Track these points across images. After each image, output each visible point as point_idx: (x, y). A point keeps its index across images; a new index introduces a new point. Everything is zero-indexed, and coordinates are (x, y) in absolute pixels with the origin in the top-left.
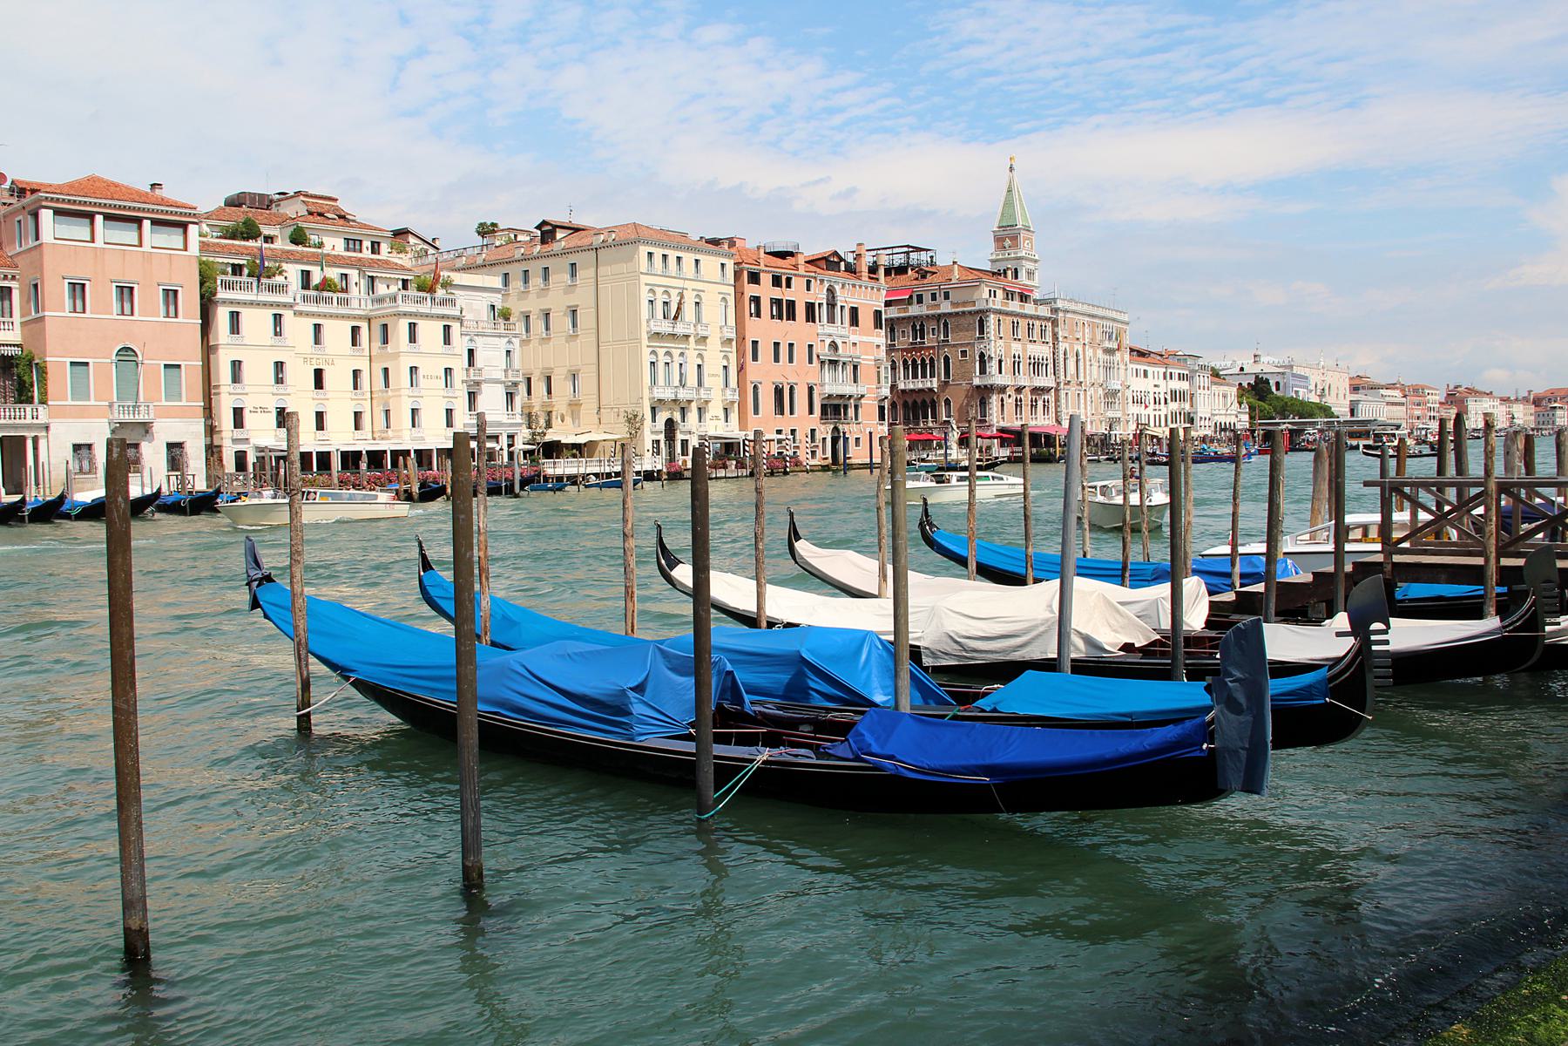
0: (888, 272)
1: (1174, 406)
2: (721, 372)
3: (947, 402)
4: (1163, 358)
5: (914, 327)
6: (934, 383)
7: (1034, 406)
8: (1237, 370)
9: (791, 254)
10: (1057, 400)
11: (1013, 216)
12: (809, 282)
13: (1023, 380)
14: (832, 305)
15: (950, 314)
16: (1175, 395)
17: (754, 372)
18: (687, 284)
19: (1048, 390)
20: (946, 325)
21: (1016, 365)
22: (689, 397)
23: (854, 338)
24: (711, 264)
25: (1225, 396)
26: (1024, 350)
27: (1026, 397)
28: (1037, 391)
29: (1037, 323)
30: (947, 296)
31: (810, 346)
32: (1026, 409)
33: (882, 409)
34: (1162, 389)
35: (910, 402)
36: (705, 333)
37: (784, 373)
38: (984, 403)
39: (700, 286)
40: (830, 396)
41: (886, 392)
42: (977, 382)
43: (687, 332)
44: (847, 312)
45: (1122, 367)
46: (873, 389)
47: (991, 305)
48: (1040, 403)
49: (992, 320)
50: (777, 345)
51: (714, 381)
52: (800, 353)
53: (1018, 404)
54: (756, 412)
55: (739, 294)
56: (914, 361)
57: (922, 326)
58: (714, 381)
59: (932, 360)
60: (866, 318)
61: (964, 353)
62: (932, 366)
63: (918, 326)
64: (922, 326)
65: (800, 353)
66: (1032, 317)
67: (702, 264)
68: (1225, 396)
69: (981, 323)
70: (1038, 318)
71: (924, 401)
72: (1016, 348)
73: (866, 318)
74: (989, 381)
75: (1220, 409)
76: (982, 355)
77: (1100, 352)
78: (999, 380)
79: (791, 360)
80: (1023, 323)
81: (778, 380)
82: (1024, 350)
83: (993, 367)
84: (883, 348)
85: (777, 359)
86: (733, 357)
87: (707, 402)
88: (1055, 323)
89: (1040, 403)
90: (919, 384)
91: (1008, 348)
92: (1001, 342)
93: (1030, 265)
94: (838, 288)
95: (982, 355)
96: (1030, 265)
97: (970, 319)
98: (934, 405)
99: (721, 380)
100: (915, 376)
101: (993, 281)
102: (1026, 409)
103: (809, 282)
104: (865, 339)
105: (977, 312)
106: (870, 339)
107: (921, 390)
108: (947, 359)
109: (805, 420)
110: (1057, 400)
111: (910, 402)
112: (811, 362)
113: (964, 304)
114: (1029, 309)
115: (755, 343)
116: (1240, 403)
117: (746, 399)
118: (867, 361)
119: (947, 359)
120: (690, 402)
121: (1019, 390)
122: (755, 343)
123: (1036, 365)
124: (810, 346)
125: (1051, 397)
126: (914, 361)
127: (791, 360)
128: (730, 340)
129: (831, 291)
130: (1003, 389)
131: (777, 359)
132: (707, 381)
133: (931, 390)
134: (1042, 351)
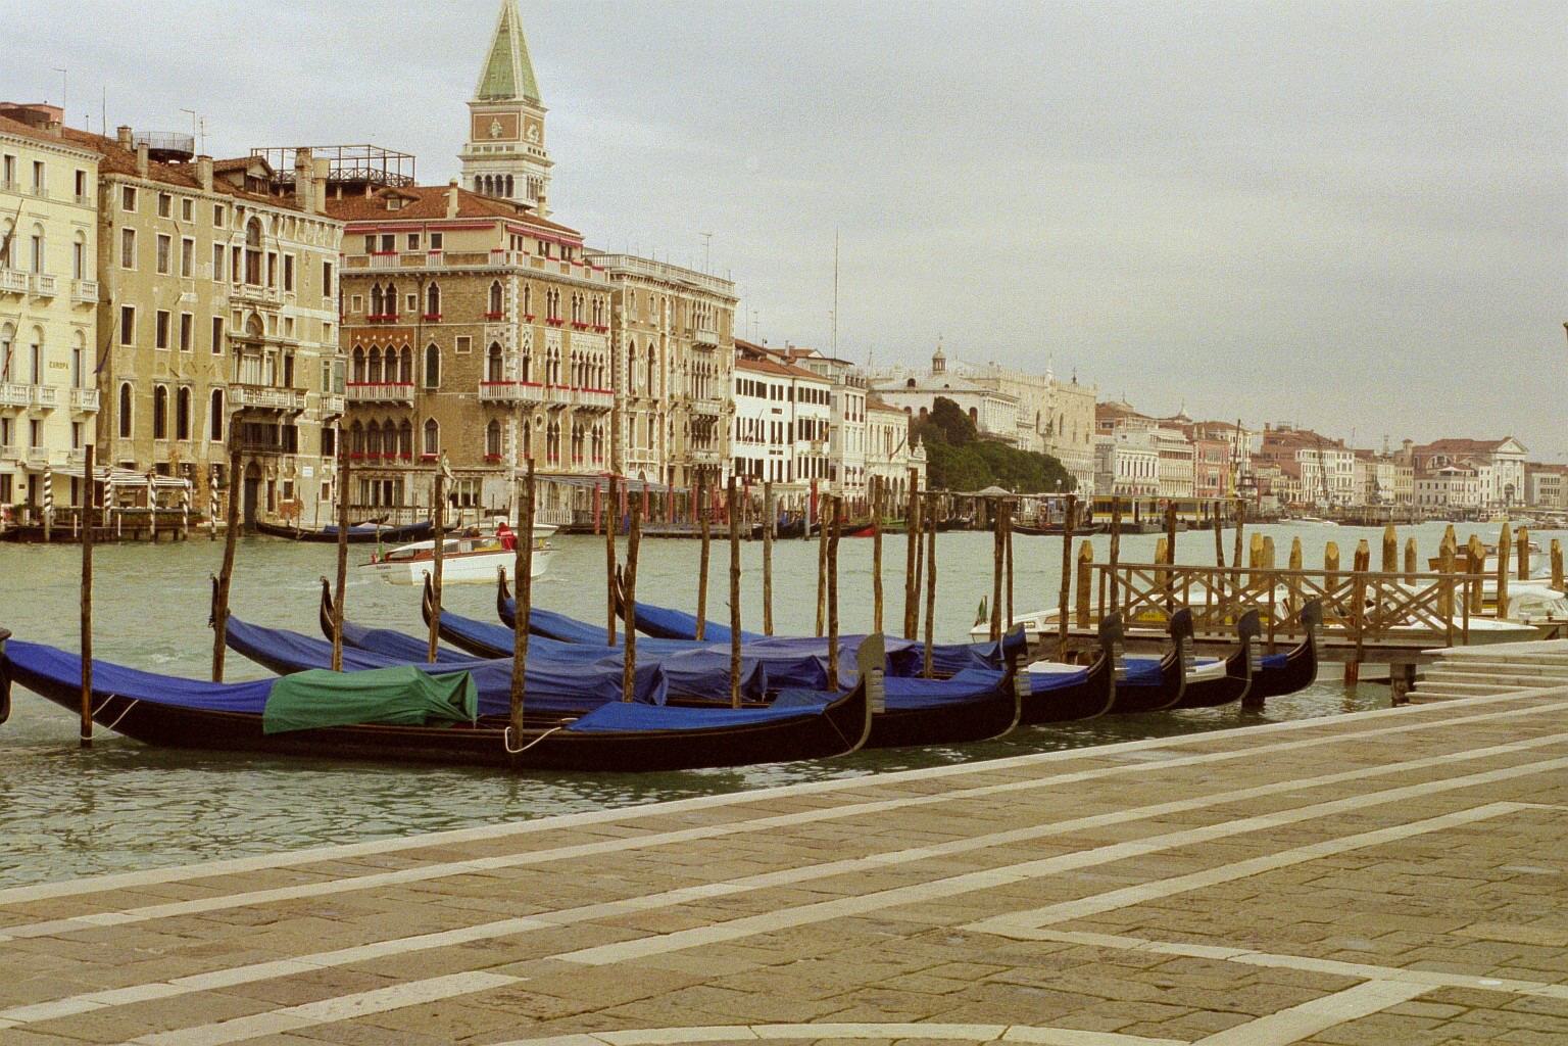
0: (331, 187)
1: (803, 446)
2: (70, 359)
3: (431, 426)
4: (789, 360)
5: (377, 291)
6: (410, 393)
7: (577, 439)
8: (902, 382)
9: (183, 156)
10: (615, 430)
11: (508, 76)
12: (219, 210)
13: (563, 397)
14: (253, 257)
15: (443, 274)
16: (807, 429)
17: (126, 364)
18: (30, 205)
19: (603, 411)
20: (434, 297)
21: (552, 364)
22: (18, 401)
23: (287, 310)
24: (61, 168)
25: (888, 433)
26: (566, 341)
27: (566, 423)
28: (583, 411)
29: (589, 296)
30: (437, 241)
31: (218, 322)
32: (565, 444)
33: (327, 434)
34: (785, 418)
35: (364, 421)
36: (47, 292)
37: (168, 367)
38: (494, 430)
39: (39, 207)
40: (248, 409)
41: (337, 404)
42: (484, 393)
43: (18, 288)
44: (280, 264)
45: (723, 377)
46: (317, 404)
47: (514, 261)
48: (588, 434)
49: (513, 288)
50: (163, 317)
51: (57, 378)
52: (201, 334)
53: (552, 435)
54: (125, 431)
55: (104, 224)
56: (374, 351)
57: (391, 289)
58: (57, 378)
59: (406, 350)
60: (307, 277)
61: (464, 342)
62: (407, 365)
63: (384, 289)
64: (391, 289)
65: (201, 334)
66: (580, 285)
67: (46, 170)
68: (888, 433)
69: (497, 291)
70: (589, 287)
71: (389, 423)
72: (553, 336)
73: (307, 277)
74: (505, 393)
75: (876, 453)
76: (495, 349)
77: (686, 349)
78: (523, 394)
79: (185, 346)
80: (564, 297)
81: (164, 378)
82: (566, 341)
83: (512, 369)
84: (335, 329)
85: (162, 343)
86: (91, 334)
87: (46, 411)
88: (617, 298)
89: (588, 434)
90: (380, 394)
91: (539, 336)
92: (528, 328)
93: (535, 170)
94: (266, 221)
95: (495, 349)
96: (535, 170)
97: (475, 285)
98: (406, 426)
99: (68, 375)
100: (375, 382)
101: (517, 224)
102: (565, 444)
103: (219, 210)
104: (307, 312)
105: (490, 274)
106: (317, 313)
107: (385, 405)
108: (433, 352)
109: (206, 449)
110: (615, 430)
111: (364, 421)
112: (217, 349)
113: (469, 257)
114: (576, 274)
115: (128, 313)
116: (912, 446)
117: (114, 412)
118: (308, 350)
119: (433, 352)
120: (18, 409)
121: (556, 409)
122: (128, 313)
123: (584, 366)
124: (218, 322)
125: (603, 423)
126: (374, 351)
127: (185, 346)
128: (87, 305)
129: (255, 225)
130: (528, 408)
131: (162, 343)
132: (48, 375)
133: (403, 404)
134: (590, 344)
